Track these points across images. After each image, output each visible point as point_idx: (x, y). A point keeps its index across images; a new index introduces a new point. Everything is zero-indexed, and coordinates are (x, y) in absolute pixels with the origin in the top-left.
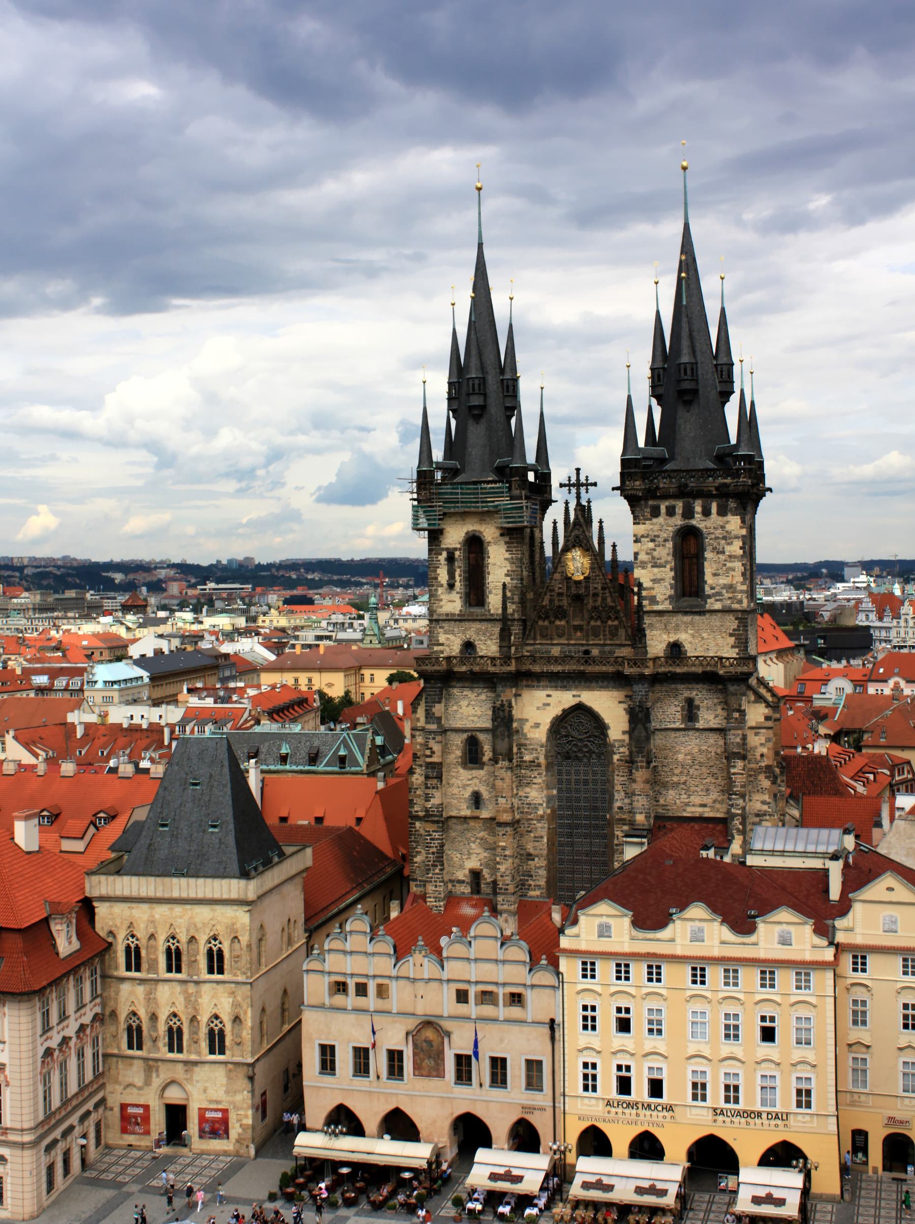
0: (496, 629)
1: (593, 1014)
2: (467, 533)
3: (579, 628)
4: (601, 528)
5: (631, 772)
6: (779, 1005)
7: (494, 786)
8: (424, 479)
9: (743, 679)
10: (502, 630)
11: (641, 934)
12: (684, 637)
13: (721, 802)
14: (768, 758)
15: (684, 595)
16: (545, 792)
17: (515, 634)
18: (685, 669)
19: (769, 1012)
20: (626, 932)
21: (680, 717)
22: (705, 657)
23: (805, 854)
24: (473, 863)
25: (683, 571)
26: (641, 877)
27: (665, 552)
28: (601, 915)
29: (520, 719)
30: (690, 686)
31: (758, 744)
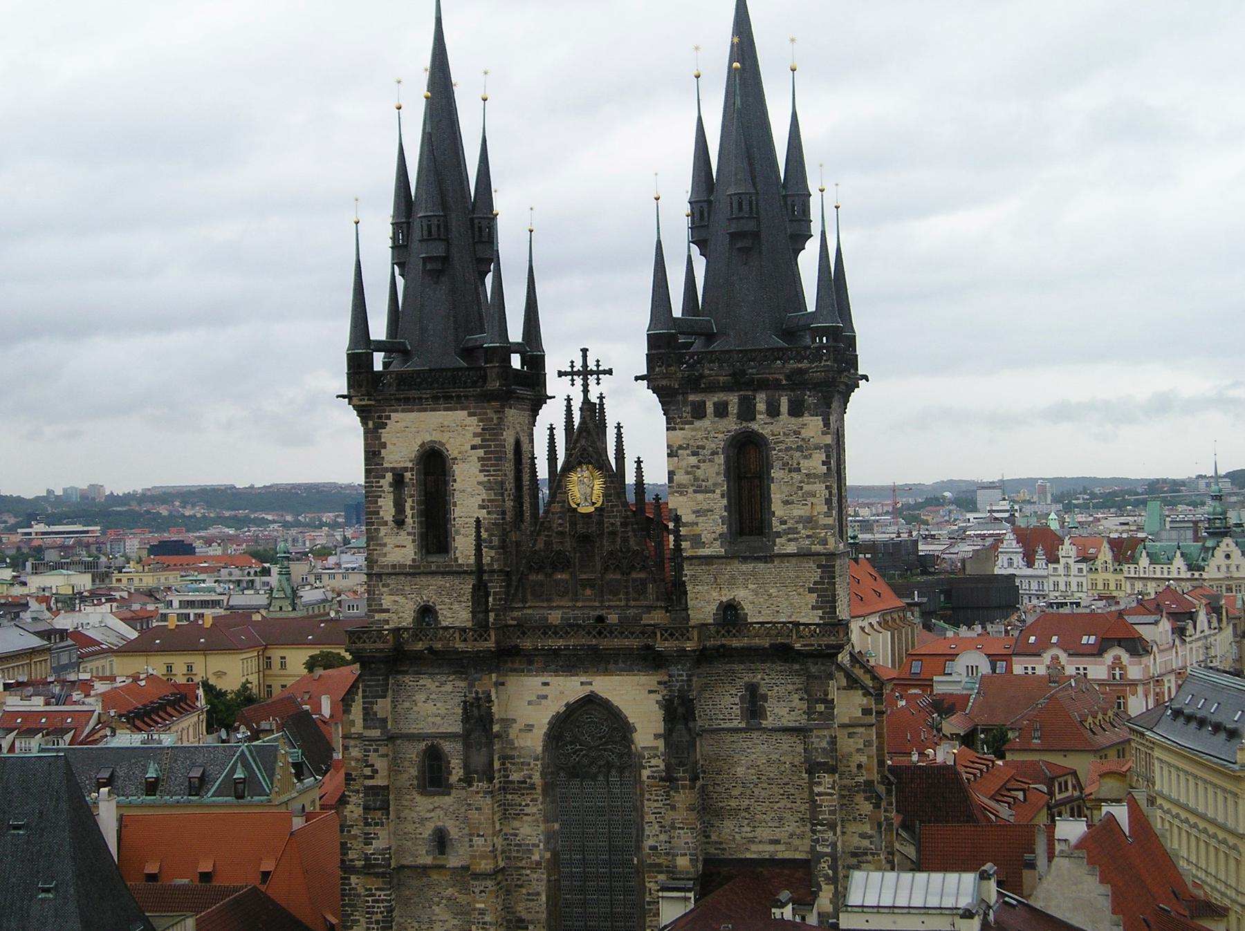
0: (468, 587)
3: (589, 584)
4: (619, 436)
8: (358, 365)
9: (828, 655)
12: (742, 594)
13: (801, 836)
14: (868, 770)
15: (741, 532)
16: (542, 827)
18: (745, 642)
27: (714, 471)
31: (853, 750)
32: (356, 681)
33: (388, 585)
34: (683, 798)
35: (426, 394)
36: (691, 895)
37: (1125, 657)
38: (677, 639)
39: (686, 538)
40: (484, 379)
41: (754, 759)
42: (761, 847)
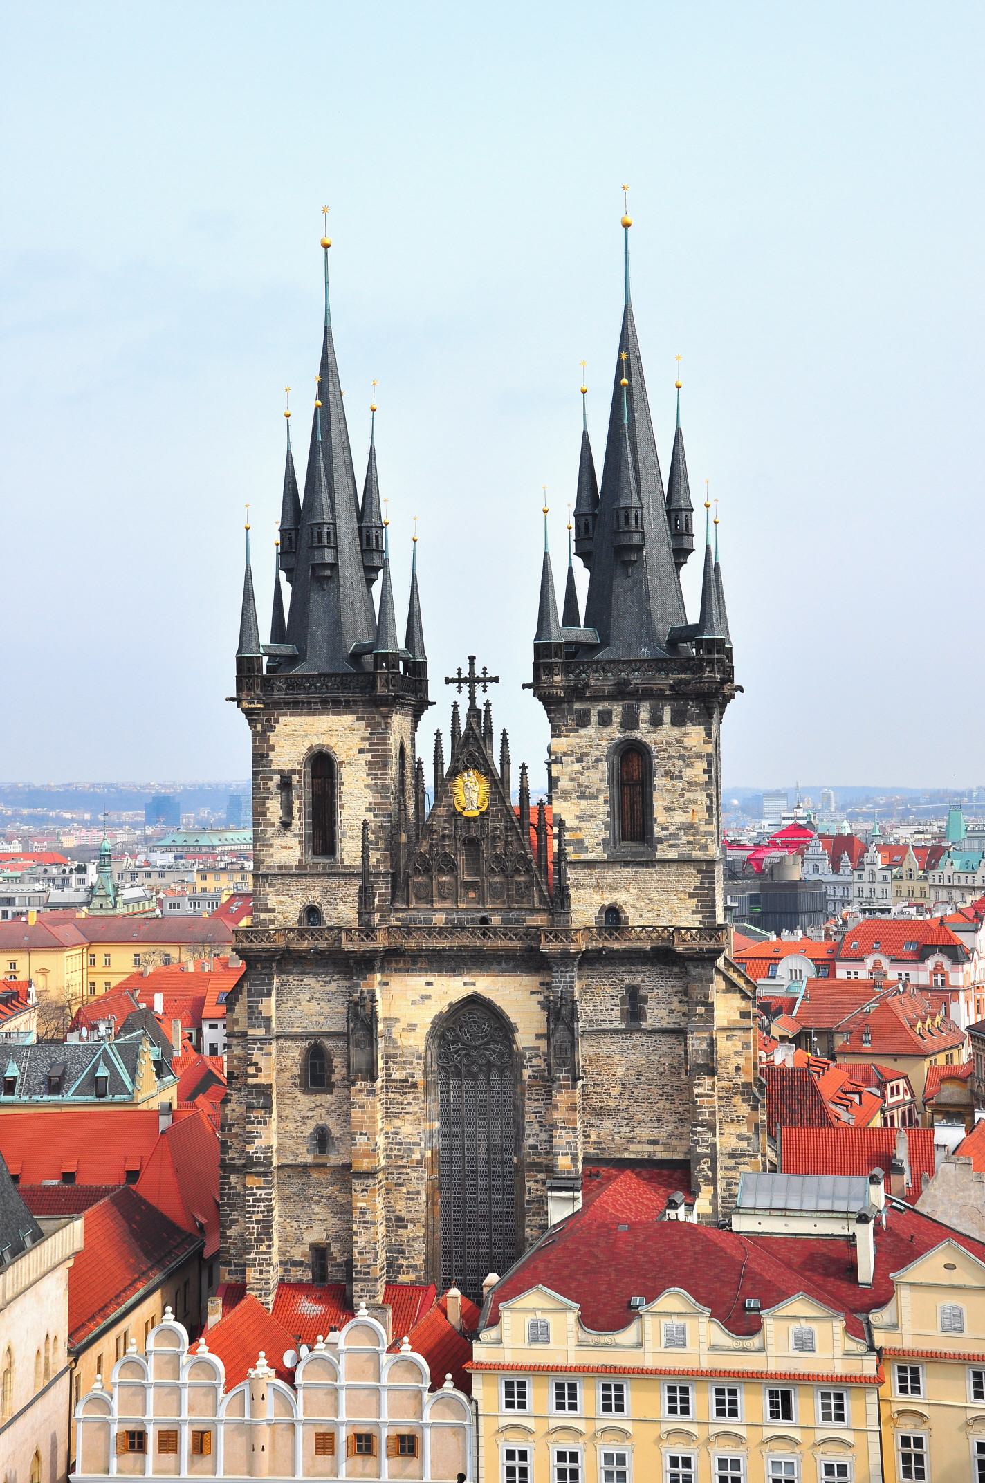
0: (354, 887)
1: (523, 1464)
2: (310, 749)
4: (505, 742)
5: (549, 1095)
6: (850, 1446)
7: (348, 1118)
8: (246, 667)
11: (591, 1337)
13: (680, 1137)
14: (746, 1072)
15: (624, 838)
19: (784, 1455)
21: (619, 1013)
22: (655, 928)
23: (817, 1213)
24: (316, 1235)
25: (622, 804)
26: (584, 1249)
27: (597, 778)
28: (534, 1310)
29: (386, 1019)
30: (633, 969)
33: (274, 886)
36: (579, 1195)
37: (947, 964)
38: (562, 941)
39: (568, 843)
40: (374, 687)
42: (639, 1148)
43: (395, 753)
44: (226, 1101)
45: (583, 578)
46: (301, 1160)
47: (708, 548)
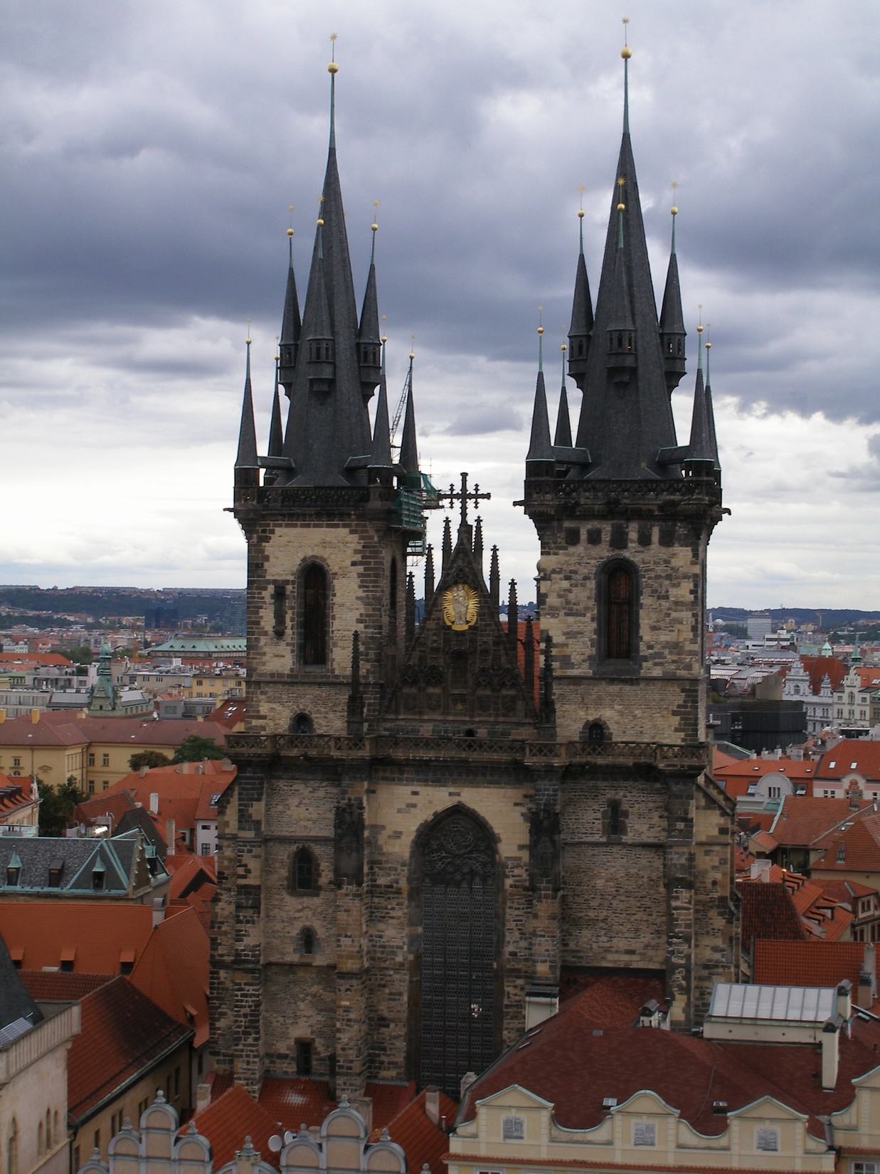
0: (344, 697)
2: (304, 560)
3: (461, 699)
5: (530, 903)
7: (334, 919)
8: (244, 478)
9: (689, 775)
10: (352, 699)
11: (564, 1132)
12: (608, 715)
13: (656, 948)
14: (723, 887)
15: (609, 655)
16: (407, 930)
17: (369, 705)
18: (609, 760)
20: (545, 1131)
24: (301, 1030)
27: (585, 595)
32: (233, 783)
34: (545, 908)
35: (312, 510)
39: (555, 659)
40: (366, 498)
41: (610, 872)
43: (387, 565)
44: (216, 900)
45: (576, 396)
46: (288, 959)
47: (699, 372)
